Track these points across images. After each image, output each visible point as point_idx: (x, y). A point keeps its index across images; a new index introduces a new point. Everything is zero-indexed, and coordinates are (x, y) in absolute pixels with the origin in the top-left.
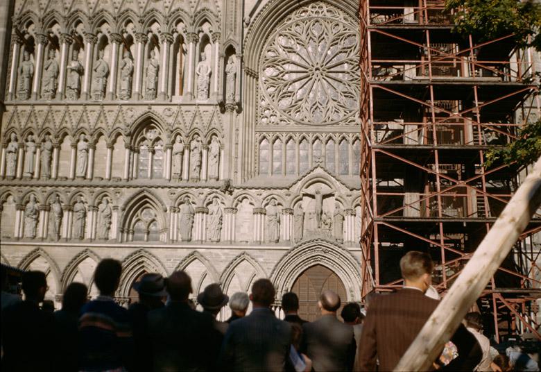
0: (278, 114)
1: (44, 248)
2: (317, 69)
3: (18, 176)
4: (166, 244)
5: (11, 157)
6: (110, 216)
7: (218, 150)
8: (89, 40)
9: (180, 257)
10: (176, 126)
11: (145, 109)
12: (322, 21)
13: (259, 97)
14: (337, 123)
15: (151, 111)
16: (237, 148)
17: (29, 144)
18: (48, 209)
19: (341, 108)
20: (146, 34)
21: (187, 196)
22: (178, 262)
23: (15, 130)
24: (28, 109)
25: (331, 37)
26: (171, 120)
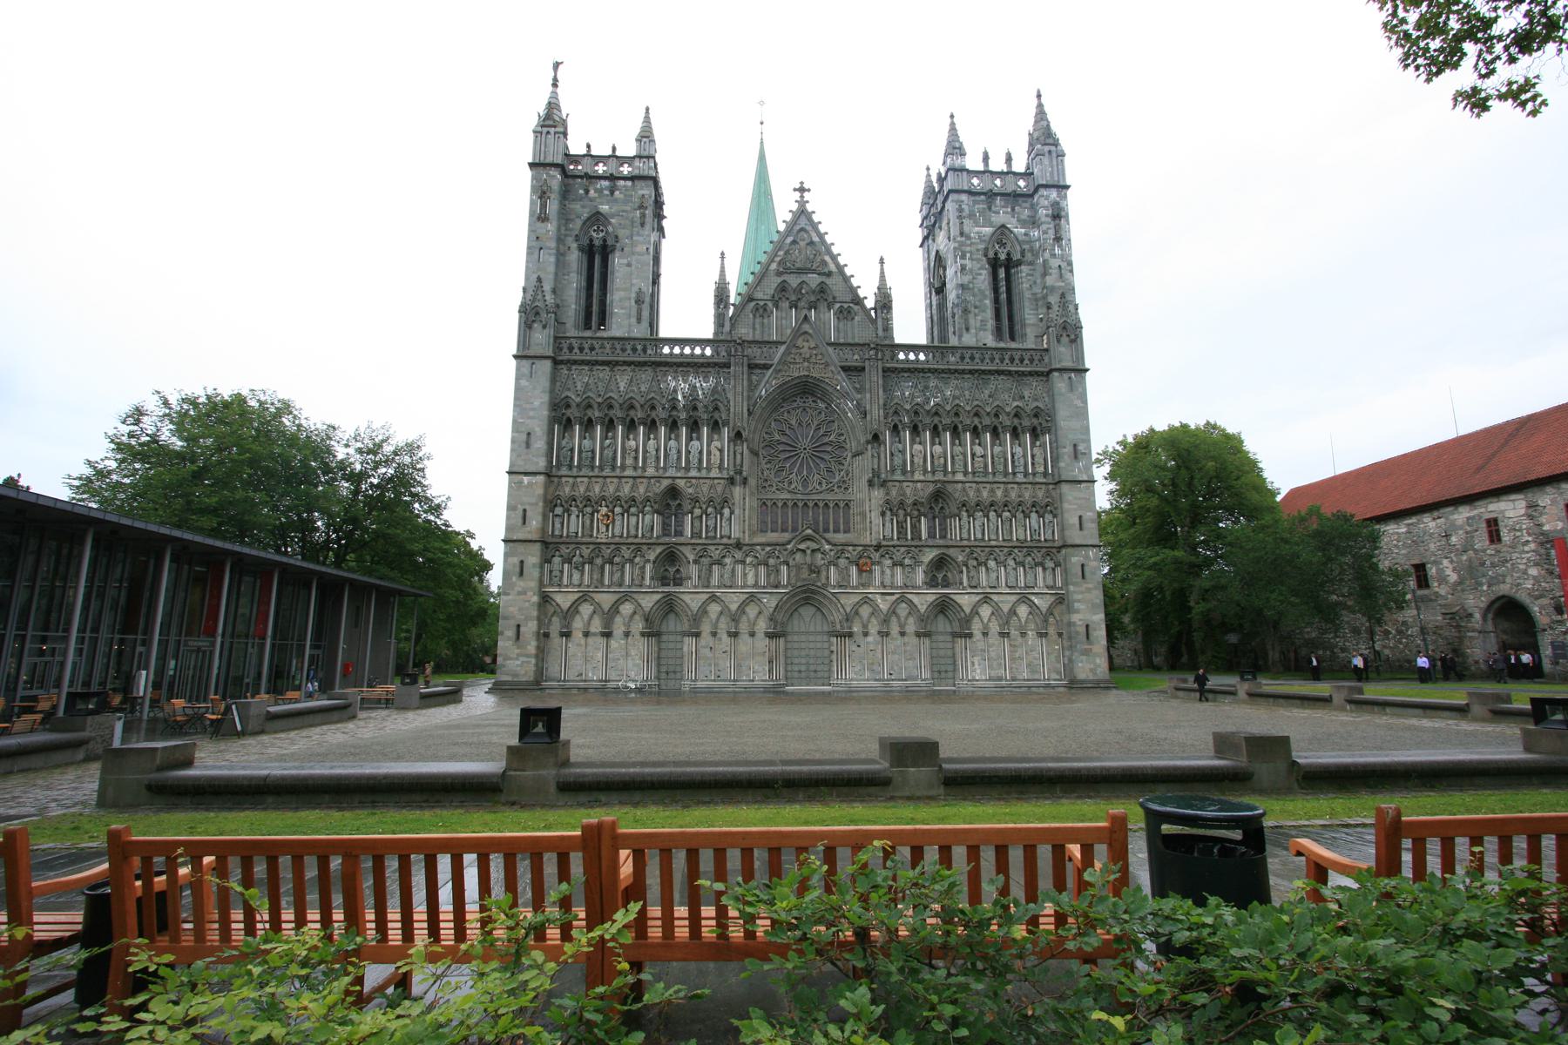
6: (644, 567)
11: (670, 481)
18: (591, 562)
24: (571, 480)
25: (816, 423)
26: (690, 490)
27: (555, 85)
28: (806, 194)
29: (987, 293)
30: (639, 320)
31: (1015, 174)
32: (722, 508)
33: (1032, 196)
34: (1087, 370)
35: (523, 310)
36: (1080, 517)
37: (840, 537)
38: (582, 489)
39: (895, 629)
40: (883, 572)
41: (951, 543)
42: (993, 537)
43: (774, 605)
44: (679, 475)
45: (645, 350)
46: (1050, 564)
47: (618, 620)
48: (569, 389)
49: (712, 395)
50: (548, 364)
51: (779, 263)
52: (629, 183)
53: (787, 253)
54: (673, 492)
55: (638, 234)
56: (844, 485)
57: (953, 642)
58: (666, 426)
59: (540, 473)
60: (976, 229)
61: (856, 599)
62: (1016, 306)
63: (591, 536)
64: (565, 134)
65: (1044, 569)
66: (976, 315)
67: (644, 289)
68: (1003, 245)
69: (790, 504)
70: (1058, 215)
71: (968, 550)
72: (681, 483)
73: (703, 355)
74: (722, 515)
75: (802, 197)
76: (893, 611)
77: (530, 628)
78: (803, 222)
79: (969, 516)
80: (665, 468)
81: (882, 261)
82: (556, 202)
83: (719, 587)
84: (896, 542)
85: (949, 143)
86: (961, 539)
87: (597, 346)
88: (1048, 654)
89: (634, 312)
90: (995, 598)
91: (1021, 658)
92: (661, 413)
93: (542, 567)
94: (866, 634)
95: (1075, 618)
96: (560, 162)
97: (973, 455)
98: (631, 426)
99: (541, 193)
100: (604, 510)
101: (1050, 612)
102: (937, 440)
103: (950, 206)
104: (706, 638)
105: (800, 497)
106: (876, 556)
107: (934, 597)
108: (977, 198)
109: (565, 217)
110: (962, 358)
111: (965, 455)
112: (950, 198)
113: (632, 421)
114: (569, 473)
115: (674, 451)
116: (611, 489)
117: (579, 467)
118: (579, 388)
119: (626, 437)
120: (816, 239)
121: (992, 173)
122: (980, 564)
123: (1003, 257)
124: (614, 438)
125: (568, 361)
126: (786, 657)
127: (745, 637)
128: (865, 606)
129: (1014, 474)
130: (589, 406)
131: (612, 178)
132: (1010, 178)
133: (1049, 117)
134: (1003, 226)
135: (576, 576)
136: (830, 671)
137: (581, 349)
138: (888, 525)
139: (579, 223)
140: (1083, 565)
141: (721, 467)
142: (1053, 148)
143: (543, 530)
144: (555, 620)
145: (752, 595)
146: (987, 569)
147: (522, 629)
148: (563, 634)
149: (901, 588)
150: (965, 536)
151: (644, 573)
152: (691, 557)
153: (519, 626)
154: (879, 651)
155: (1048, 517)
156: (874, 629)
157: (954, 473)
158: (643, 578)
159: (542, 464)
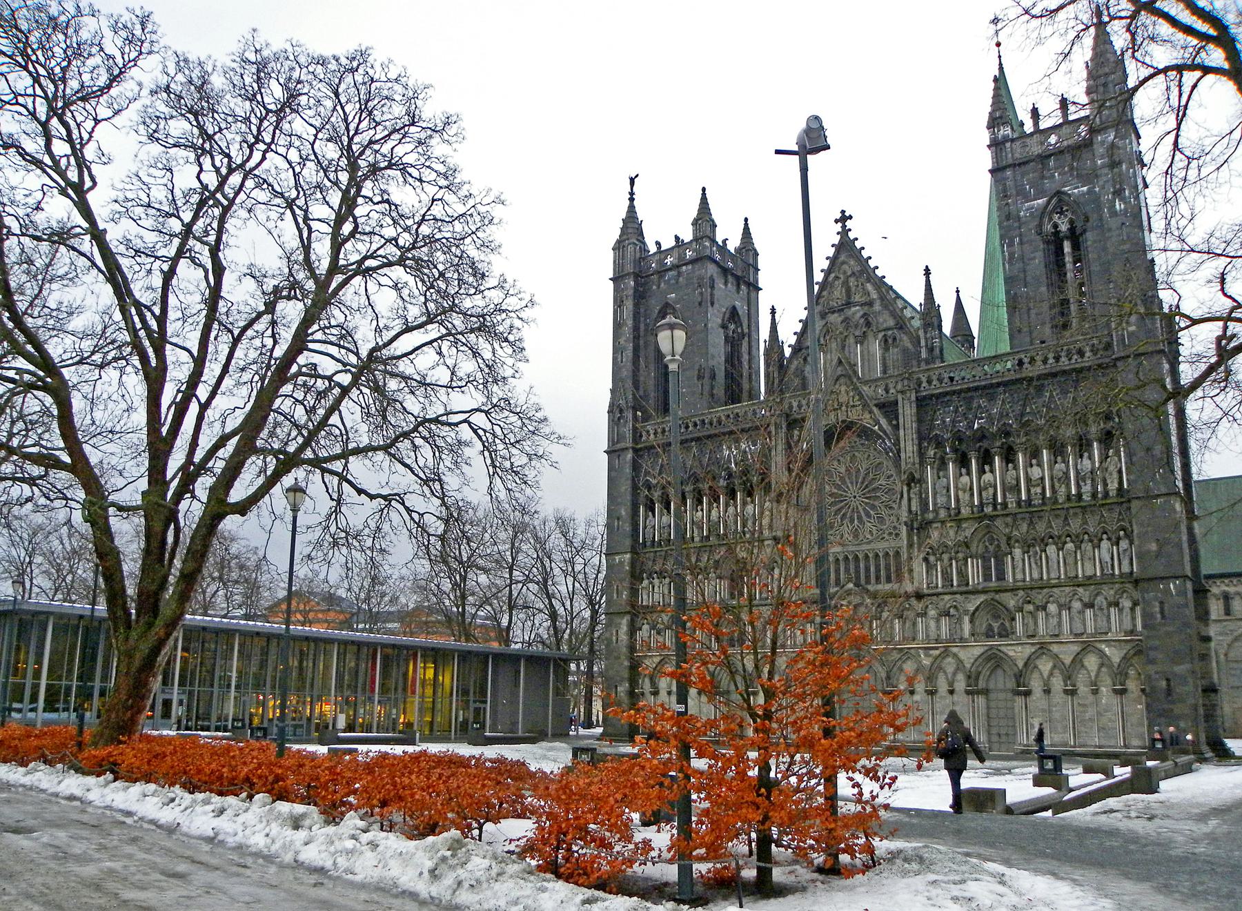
27: (632, 200)
28: (849, 224)
32: (773, 569)
37: (885, 587)
52: (690, 267)
57: (1014, 701)
65: (1121, 611)
75: (844, 226)
81: (927, 272)
84: (940, 590)
97: (1028, 480)
102: (987, 468)
105: (851, 548)
106: (919, 606)
107: (982, 650)
123: (1064, 228)
131: (676, 267)
132: (1066, 130)
141: (771, 527)
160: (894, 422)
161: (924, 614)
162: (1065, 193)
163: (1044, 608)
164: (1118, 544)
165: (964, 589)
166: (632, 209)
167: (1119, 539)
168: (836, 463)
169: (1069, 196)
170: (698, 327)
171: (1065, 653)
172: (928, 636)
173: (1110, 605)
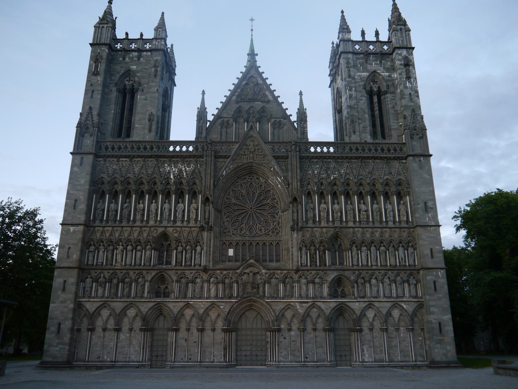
0: (231, 231)
1: (108, 302)
2: (251, 208)
3: (95, 264)
4: (173, 299)
5: (91, 255)
6: (144, 285)
7: (200, 251)
8: (134, 193)
9: (180, 306)
10: (180, 238)
11: (163, 229)
12: (253, 183)
13: (222, 222)
14: (261, 236)
15: (166, 230)
16: (210, 249)
17: (101, 247)
19: (263, 228)
20: (164, 189)
21: (184, 274)
22: (179, 309)
23: (93, 240)
24: (101, 229)
25: (258, 192)
26: (176, 235)
29: (366, 110)
30: (150, 131)
31: (381, 42)
32: (197, 246)
33: (392, 54)
34: (431, 155)
35: (80, 126)
36: (431, 250)
37: (274, 264)
38: (108, 235)
39: (309, 327)
40: (300, 288)
41: (346, 268)
42: (374, 263)
43: (227, 310)
44: (169, 225)
45: (152, 148)
46: (412, 281)
47: (126, 320)
48: (104, 173)
49: (192, 175)
50: (91, 157)
51: (238, 96)
52: (149, 53)
53: (242, 90)
54: (165, 236)
55: (153, 81)
56: (276, 231)
58: (163, 195)
59: (81, 224)
60: (358, 74)
61: (282, 306)
62: (385, 118)
63: (112, 265)
64: (114, 28)
65: (409, 285)
66: (359, 124)
67: (154, 112)
68: (374, 82)
69: (241, 244)
70: (408, 64)
71: (357, 272)
72: (171, 230)
73: (187, 151)
74: (195, 251)
76: (307, 314)
77: (67, 325)
78: (252, 72)
79: (357, 250)
80: (161, 221)
82: (104, 64)
83: (192, 299)
84: (309, 268)
85: (341, 26)
86: (353, 265)
87: (122, 147)
88: (414, 343)
89: (147, 126)
90: (377, 304)
91: (396, 346)
92: (159, 187)
93: (78, 285)
94: (290, 330)
95: (432, 318)
96: (108, 42)
97: (359, 211)
98: (141, 196)
99: (95, 59)
100: (121, 247)
101: (415, 314)
102: (336, 201)
103: (342, 61)
104: (183, 333)
106: (296, 277)
107: (335, 304)
108: (358, 56)
109: (109, 72)
110: (351, 150)
111: (354, 210)
112: (342, 57)
113: (142, 192)
114: (101, 225)
115: (167, 210)
116: (126, 235)
117: (107, 221)
118: (110, 172)
119: (137, 202)
120: (260, 82)
121: (367, 42)
122: (365, 282)
123: (375, 89)
124: (130, 203)
125: (104, 156)
126: (237, 346)
127: (208, 333)
128: (289, 311)
129: (387, 222)
130: (116, 183)
133: (400, 11)
134: (375, 72)
135: (100, 291)
136: (266, 355)
137: (113, 148)
138: (304, 256)
139: (118, 76)
140: (435, 282)
141: (196, 220)
142: (403, 27)
143: (80, 261)
144: (85, 320)
145: (213, 303)
146: (371, 285)
147: (62, 326)
148: (89, 330)
149: (313, 298)
150: (355, 263)
151: (144, 289)
152: (175, 278)
153: (60, 324)
154: (299, 341)
155: (411, 250)
156: (295, 326)
157: (347, 222)
158: (143, 292)
159: (82, 218)
160: (284, 168)
161: (298, 282)
162: (378, 73)
163: (370, 282)
164: (407, 250)
165: (322, 268)
166: (109, 8)
167: (408, 246)
168: (239, 186)
169: (380, 75)
170: (152, 90)
171: (382, 307)
172: (300, 295)
173: (404, 282)
